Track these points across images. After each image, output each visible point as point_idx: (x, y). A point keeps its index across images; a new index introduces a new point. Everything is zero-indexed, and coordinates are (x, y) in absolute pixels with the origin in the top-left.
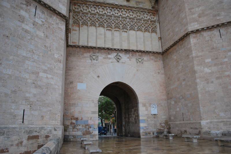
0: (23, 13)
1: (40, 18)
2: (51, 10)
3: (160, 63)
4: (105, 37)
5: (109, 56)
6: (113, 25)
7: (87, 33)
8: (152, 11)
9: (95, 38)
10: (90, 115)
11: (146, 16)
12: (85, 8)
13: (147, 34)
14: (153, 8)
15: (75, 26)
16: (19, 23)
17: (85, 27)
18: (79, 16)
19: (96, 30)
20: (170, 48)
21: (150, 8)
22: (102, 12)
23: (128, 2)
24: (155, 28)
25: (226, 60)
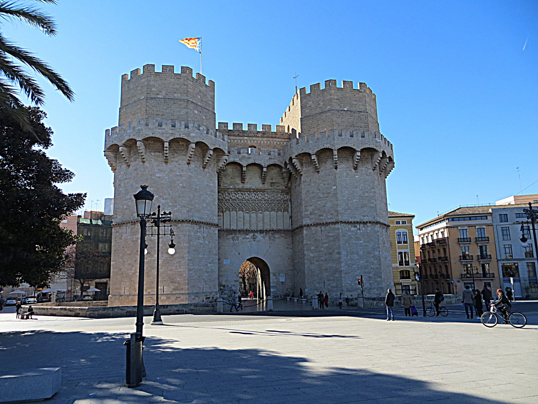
0: (199, 234)
3: (289, 239)
5: (247, 236)
9: (236, 221)
10: (233, 283)
11: (279, 195)
12: (227, 195)
14: (286, 187)
16: (197, 241)
17: (228, 212)
25: (322, 249)
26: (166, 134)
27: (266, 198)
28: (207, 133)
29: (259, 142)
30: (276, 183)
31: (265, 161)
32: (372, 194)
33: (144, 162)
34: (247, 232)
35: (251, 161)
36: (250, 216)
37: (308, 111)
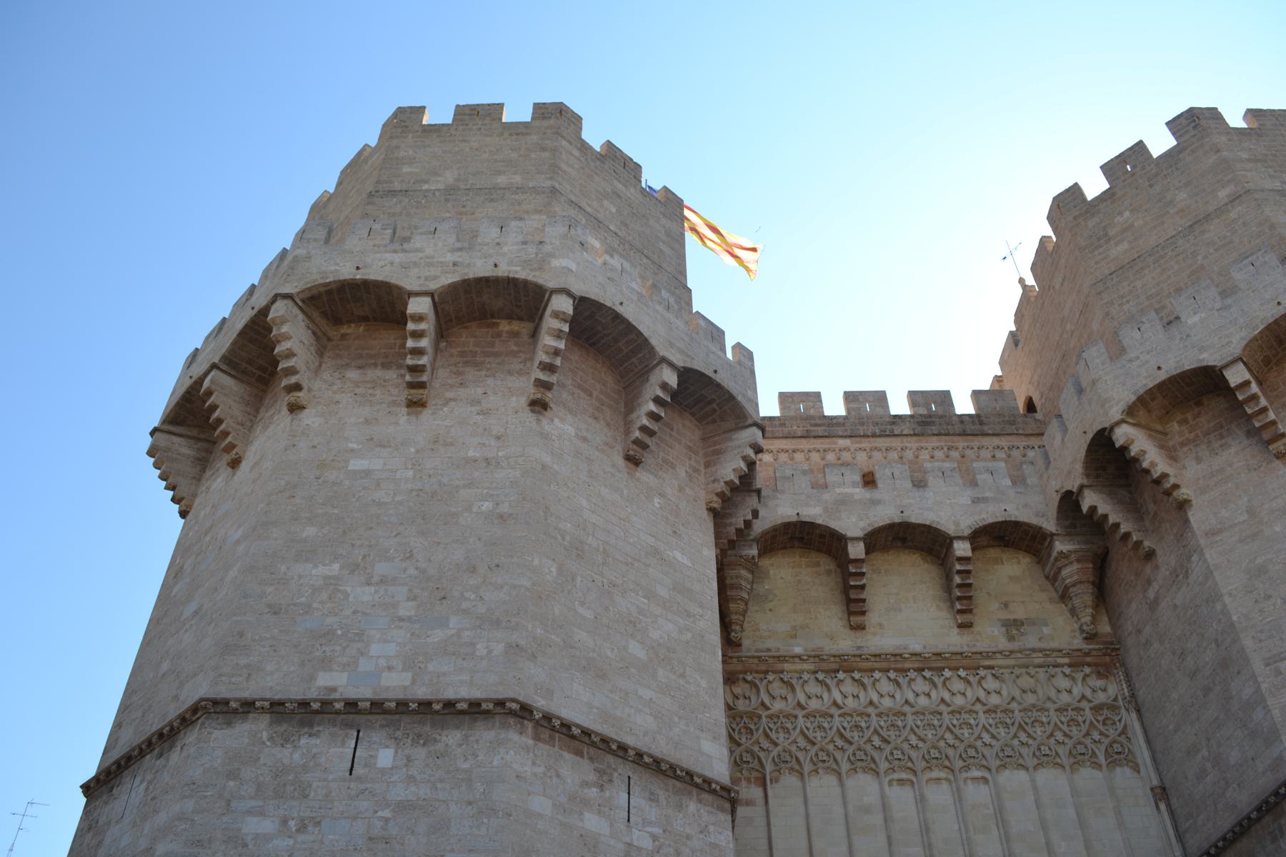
0: (592, 822)
1: (647, 823)
2: (677, 778)
6: (913, 754)
7: (802, 809)
8: (1087, 654)
11: (1063, 683)
12: (777, 689)
13: (1089, 777)
14: (1090, 637)
15: (744, 783)
17: (789, 780)
18: (757, 730)
19: (838, 790)
20: (1224, 848)
21: (1078, 643)
22: (856, 697)
23: (966, 631)
24: (1122, 739)
26: (423, 263)
27: (994, 700)
29: (909, 455)
30: (1032, 622)
31: (952, 508)
33: (295, 408)
35: (885, 514)
36: (921, 801)
37: (1125, 246)
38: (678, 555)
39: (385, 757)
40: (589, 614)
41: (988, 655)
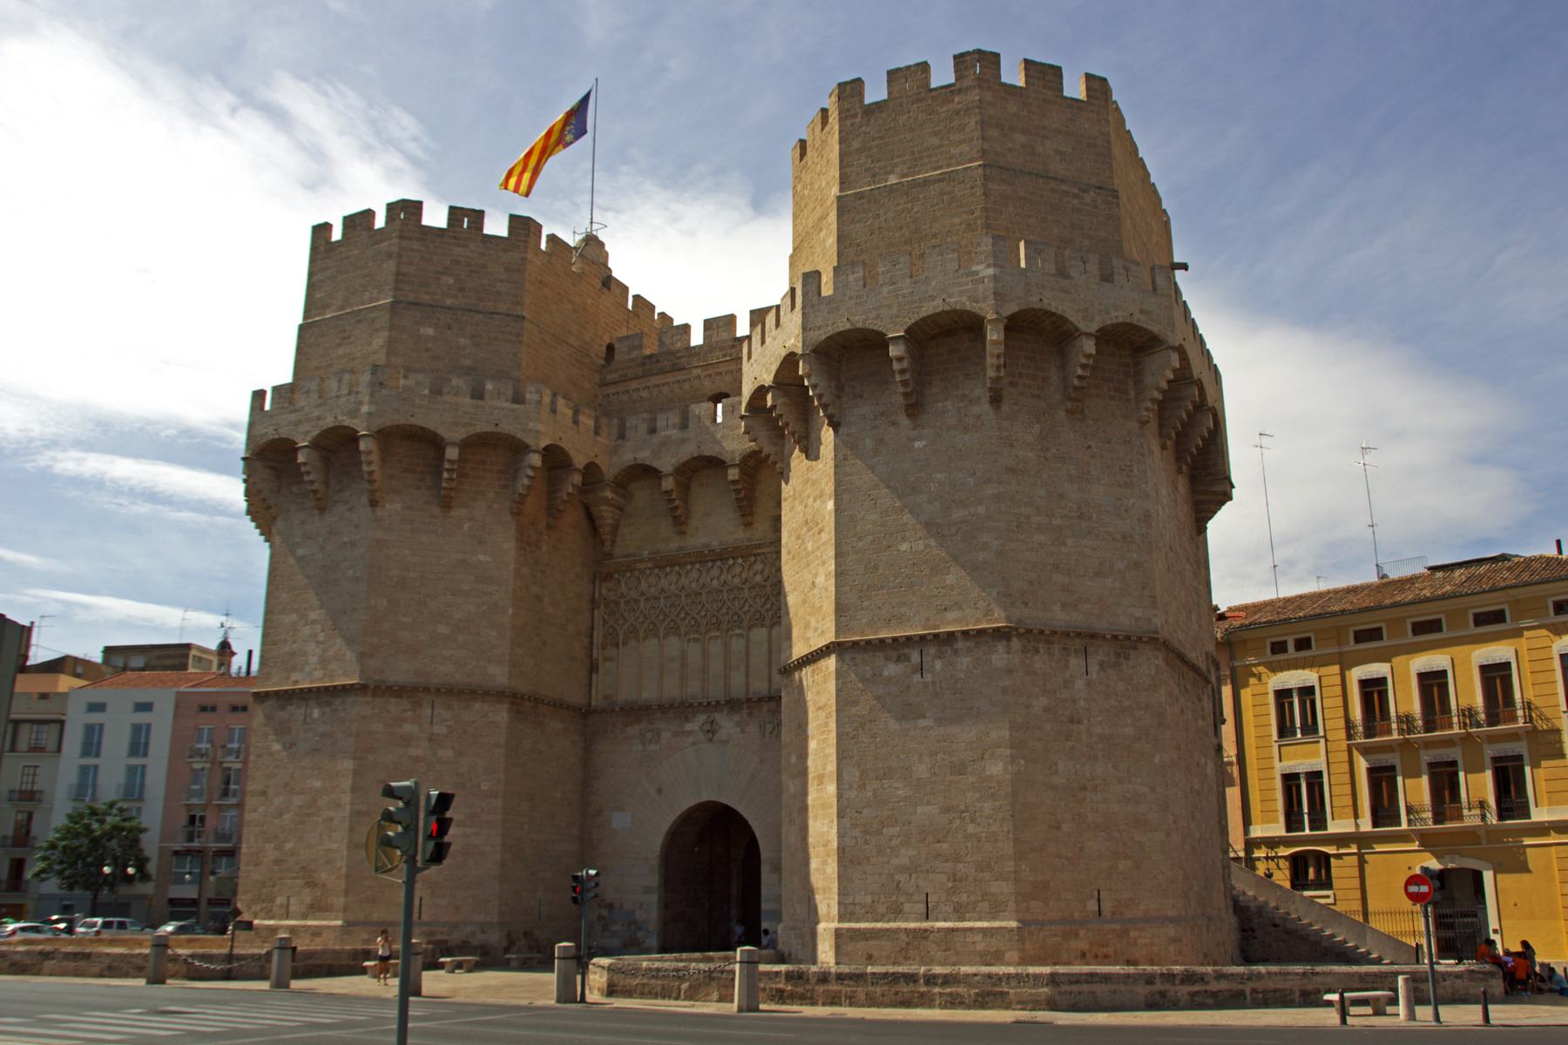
0: (408, 728)
4: (684, 664)
5: (688, 726)
17: (633, 643)
27: (759, 578)
28: (436, 391)
32: (981, 510)
34: (683, 709)
38: (482, 557)
39: (316, 713)
40: (408, 620)
41: (760, 546)
